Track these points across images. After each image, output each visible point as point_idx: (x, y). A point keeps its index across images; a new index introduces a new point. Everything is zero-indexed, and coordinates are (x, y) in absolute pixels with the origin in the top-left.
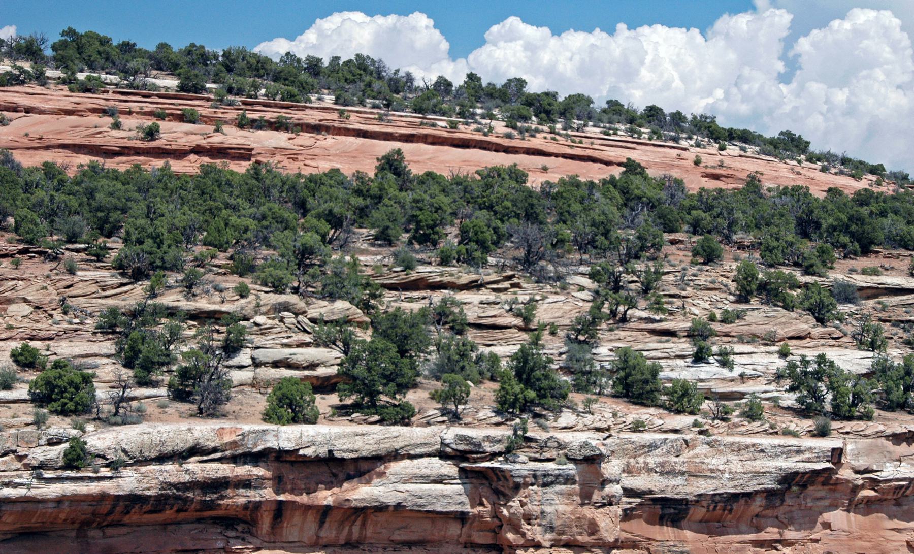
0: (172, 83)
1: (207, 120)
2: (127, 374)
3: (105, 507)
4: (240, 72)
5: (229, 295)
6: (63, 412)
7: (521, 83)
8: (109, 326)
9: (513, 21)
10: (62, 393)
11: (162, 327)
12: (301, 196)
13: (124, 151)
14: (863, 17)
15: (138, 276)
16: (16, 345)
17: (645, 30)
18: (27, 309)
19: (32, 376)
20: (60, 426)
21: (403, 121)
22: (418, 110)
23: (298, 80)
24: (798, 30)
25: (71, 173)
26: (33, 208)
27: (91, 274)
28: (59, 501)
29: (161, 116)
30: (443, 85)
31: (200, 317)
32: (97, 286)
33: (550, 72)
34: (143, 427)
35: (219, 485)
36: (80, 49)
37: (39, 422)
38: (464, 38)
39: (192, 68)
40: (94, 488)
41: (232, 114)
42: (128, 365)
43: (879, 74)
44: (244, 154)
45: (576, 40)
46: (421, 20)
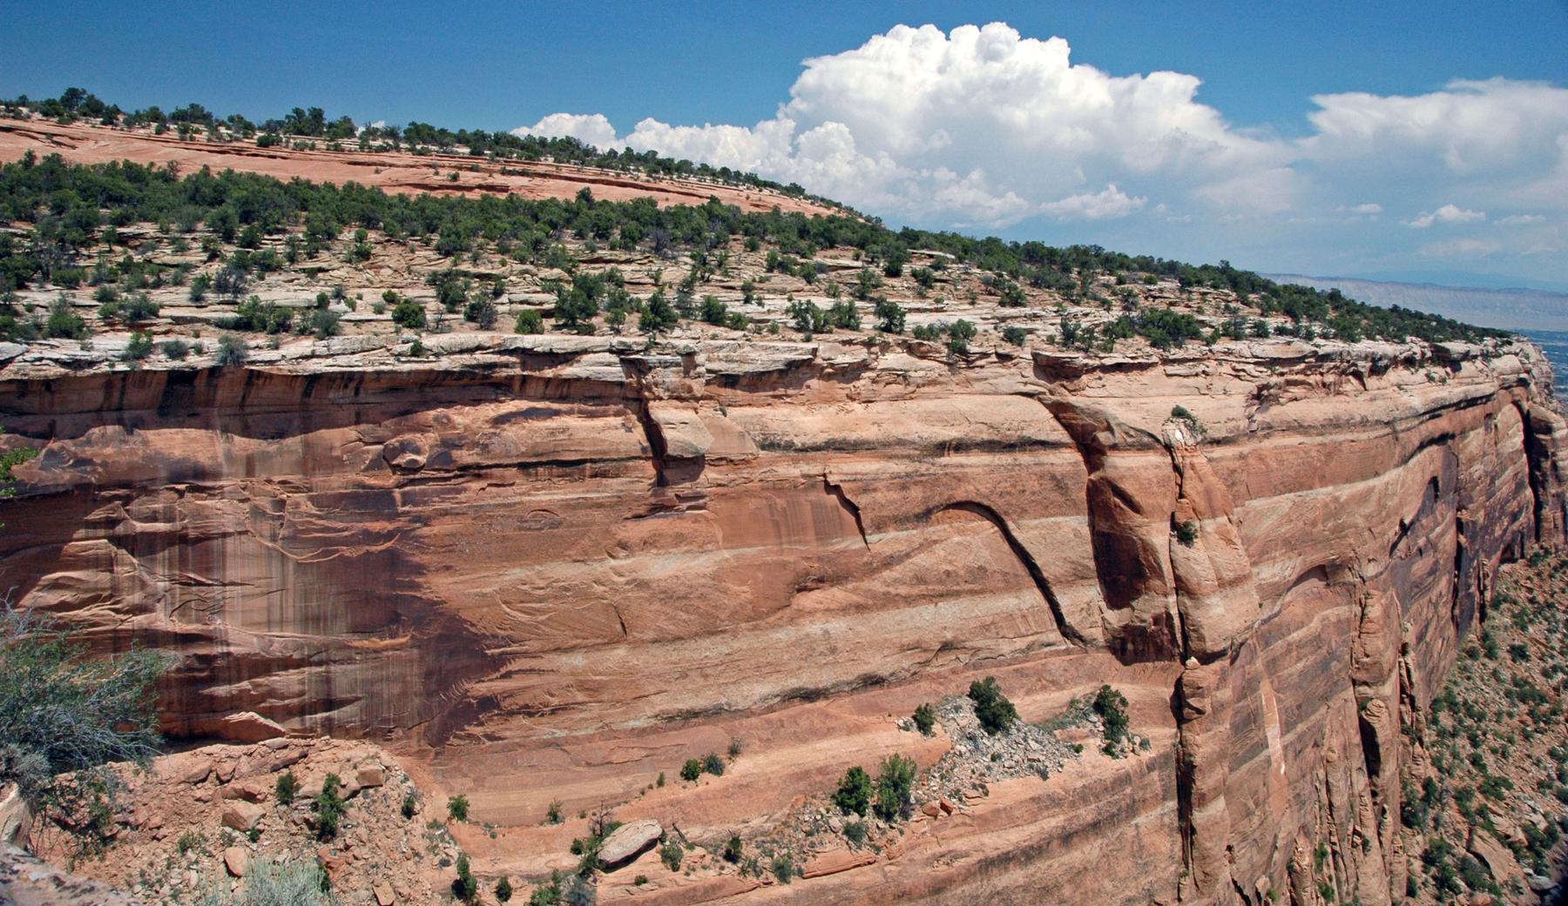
0: (466, 150)
1: (485, 171)
2: (443, 307)
3: (433, 376)
4: (503, 144)
5: (497, 265)
6: (410, 327)
7: (655, 153)
8: (433, 280)
9: (650, 121)
10: (409, 316)
11: (461, 282)
12: (535, 212)
13: (441, 187)
14: (831, 126)
15: (447, 254)
16: (385, 290)
17: (720, 127)
18: (390, 272)
19: (393, 307)
20: (408, 334)
21: (591, 172)
22: (599, 166)
23: (534, 149)
24: (799, 130)
25: (413, 199)
26: (393, 217)
27: (423, 253)
28: (409, 373)
29: (460, 168)
30: (613, 153)
31: (481, 277)
32: (427, 259)
33: (669, 148)
34: (451, 335)
35: (492, 366)
36: (418, 133)
37: (398, 331)
38: (624, 127)
39: (477, 142)
40: (427, 366)
41: (499, 167)
42: (443, 302)
43: (838, 156)
44: (504, 189)
45: (683, 131)
46: (600, 118)
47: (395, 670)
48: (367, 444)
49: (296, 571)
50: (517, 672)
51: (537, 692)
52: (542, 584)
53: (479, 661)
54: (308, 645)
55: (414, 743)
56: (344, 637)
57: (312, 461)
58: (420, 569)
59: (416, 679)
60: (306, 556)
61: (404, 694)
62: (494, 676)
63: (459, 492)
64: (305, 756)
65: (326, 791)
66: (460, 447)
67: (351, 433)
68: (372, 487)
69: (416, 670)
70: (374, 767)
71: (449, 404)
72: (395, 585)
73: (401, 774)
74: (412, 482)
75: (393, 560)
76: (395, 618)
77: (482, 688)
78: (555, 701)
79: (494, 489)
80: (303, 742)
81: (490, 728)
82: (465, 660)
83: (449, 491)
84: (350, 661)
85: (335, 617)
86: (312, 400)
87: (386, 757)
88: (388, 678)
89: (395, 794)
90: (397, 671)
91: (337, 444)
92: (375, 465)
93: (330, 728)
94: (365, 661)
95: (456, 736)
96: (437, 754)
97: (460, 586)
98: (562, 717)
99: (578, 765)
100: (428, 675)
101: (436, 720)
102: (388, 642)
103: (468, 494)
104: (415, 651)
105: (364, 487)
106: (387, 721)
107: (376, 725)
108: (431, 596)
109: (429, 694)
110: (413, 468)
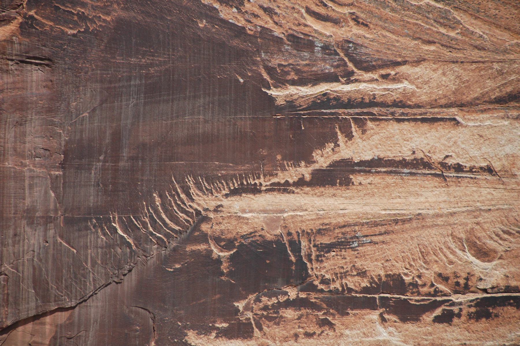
50: (371, 166)
59: (32, 168)
62: (291, 174)
77: (252, 212)
82: (197, 117)
100: (75, 157)
101: (96, 308)
104: (36, 75)
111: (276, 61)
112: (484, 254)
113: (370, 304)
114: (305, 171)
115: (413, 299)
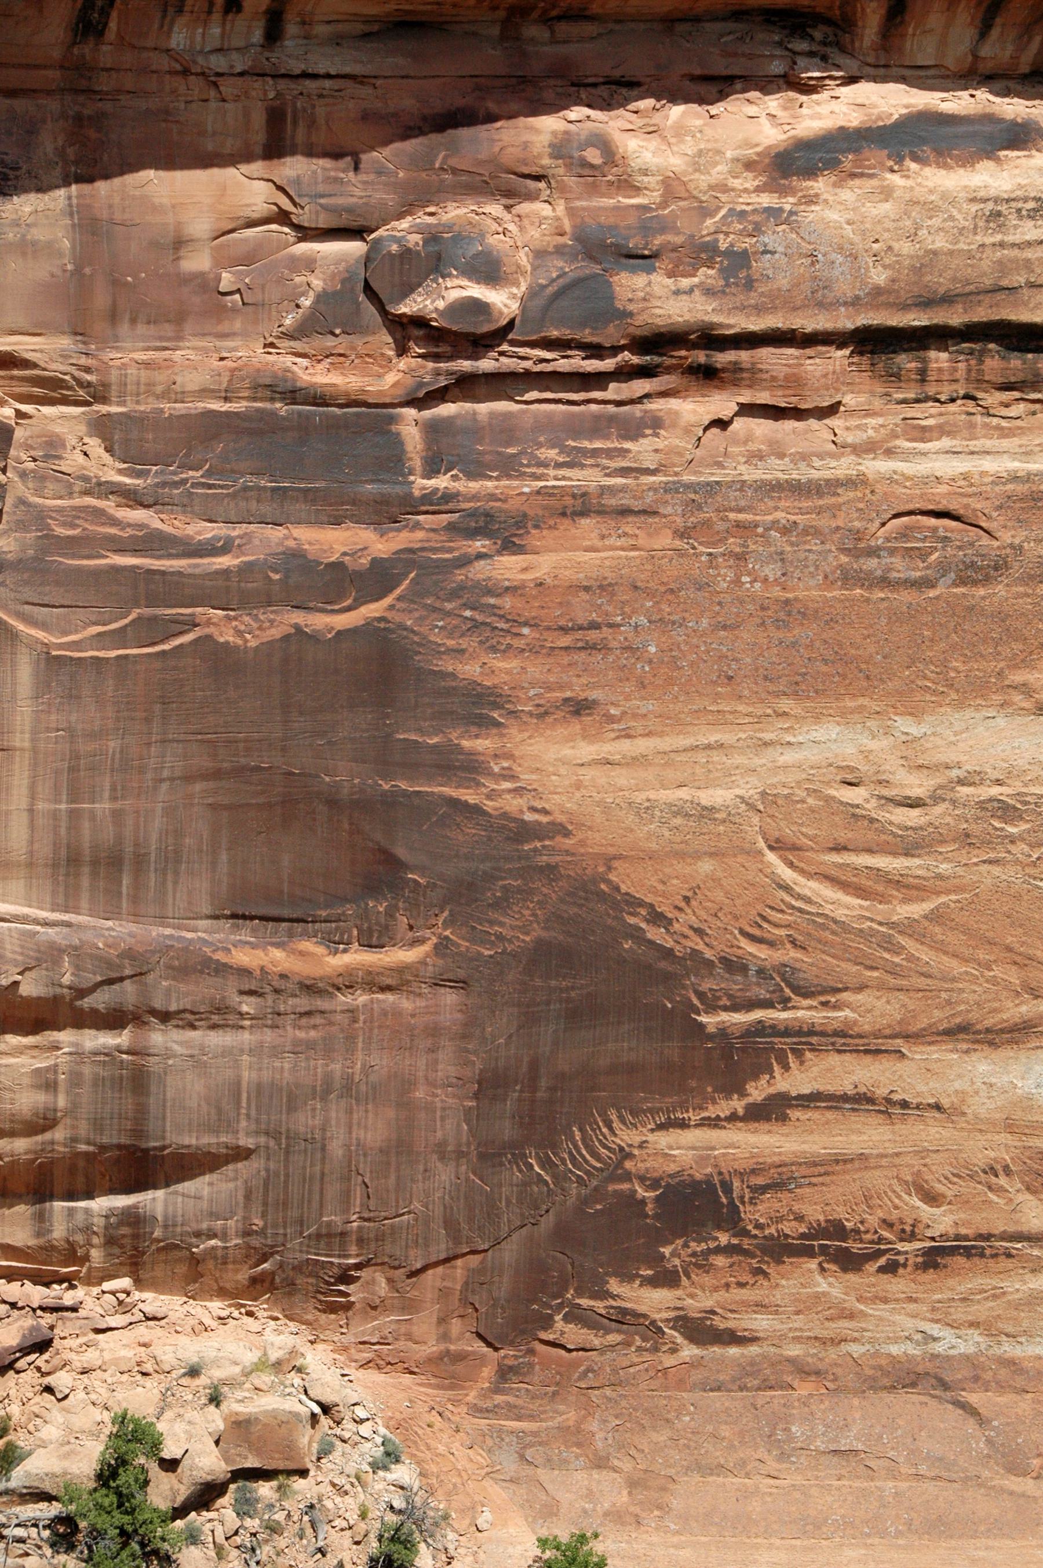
47: (375, 1061)
48: (305, 233)
49: (42, 686)
50: (810, 1100)
51: (876, 1179)
52: (917, 786)
53: (672, 1050)
54: (76, 952)
55: (424, 1324)
56: (204, 934)
57: (107, 291)
58: (481, 707)
59: (444, 1098)
60: (79, 635)
61: (400, 1148)
62: (723, 1108)
63: (633, 431)
64: (42, 1346)
65: (107, 1476)
66: (641, 259)
67: (249, 187)
68: (319, 399)
69: (447, 1067)
70: (280, 1401)
71: (614, 90)
72: (387, 756)
73: (375, 1434)
74: (466, 386)
75: (383, 669)
76: (382, 874)
77: (680, 1149)
78: (941, 1221)
79: (761, 427)
80: (37, 1294)
81: (698, 1298)
82: (621, 1044)
83: (597, 427)
84: (218, 1015)
85: (172, 859)
86: (106, 54)
87: (325, 1369)
88: (348, 1087)
89: (349, 1506)
90: (381, 1062)
91: (200, 226)
92: (326, 320)
93: (135, 1251)
94: (274, 1019)
95: (576, 1316)
96: (504, 1373)
97: (622, 778)
98: (965, 1281)
99: (1016, 1469)
100: (489, 1086)
101: (510, 1252)
102: (356, 957)
103: (667, 440)
104: (450, 998)
105: (293, 394)
106: (333, 1238)
107: (296, 1251)
108: (513, 804)
109: (490, 1155)
110: (462, 337)
111: (707, 985)
112: (932, 1198)
113: (808, 1252)
114: (738, 1105)
115: (855, 1247)
